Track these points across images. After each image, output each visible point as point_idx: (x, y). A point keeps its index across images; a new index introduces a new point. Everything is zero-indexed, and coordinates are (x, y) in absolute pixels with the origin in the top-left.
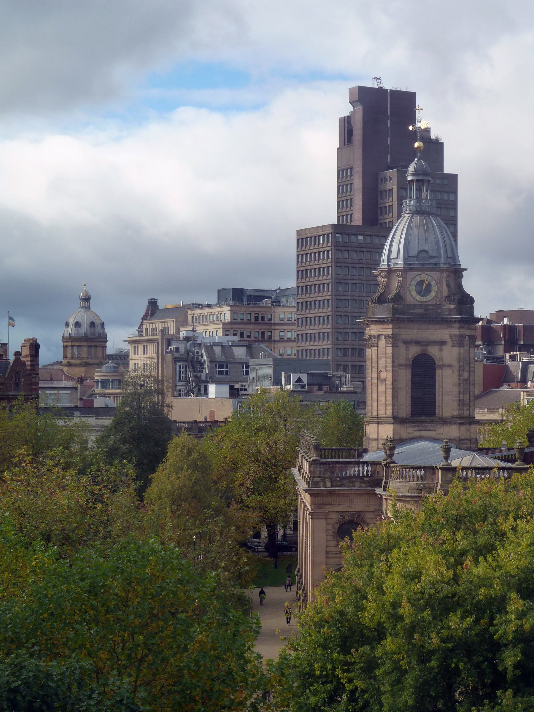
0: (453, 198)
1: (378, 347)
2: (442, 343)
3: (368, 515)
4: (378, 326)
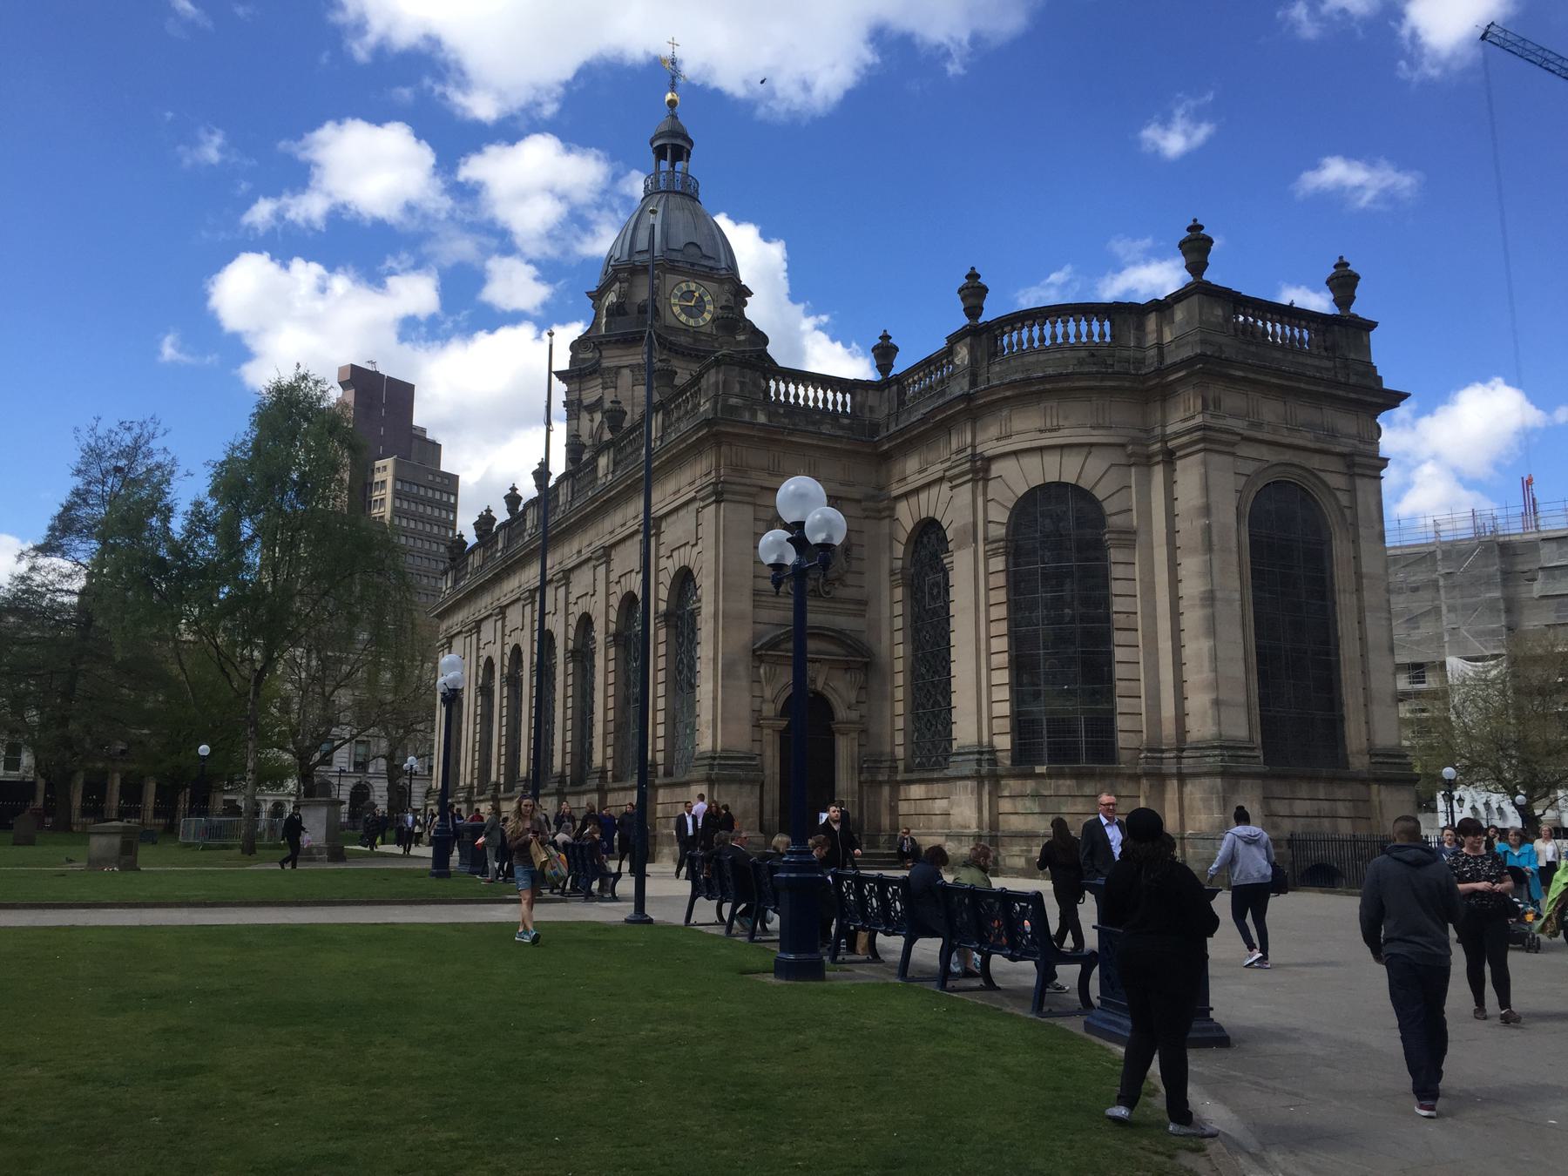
0: (452, 500)
1: (616, 388)
4: (617, 352)
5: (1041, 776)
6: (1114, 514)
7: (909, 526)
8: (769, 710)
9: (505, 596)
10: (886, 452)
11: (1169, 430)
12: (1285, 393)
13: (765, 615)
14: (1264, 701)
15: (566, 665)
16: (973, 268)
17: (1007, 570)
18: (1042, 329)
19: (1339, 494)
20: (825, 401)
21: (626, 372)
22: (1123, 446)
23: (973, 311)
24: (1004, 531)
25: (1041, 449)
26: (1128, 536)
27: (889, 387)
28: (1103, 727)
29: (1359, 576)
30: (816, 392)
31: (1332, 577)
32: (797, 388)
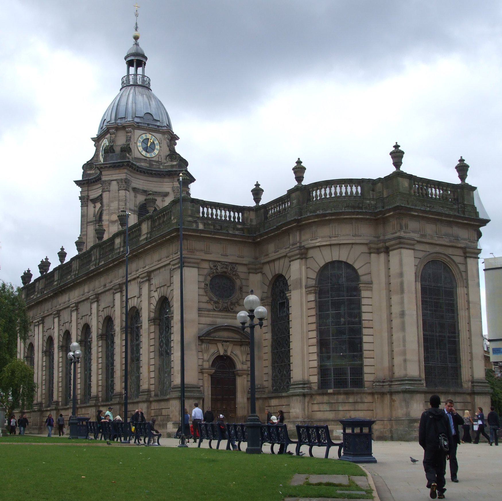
3: (241, 269)
5: (330, 394)
6: (363, 275)
7: (270, 277)
8: (206, 365)
9: (60, 305)
10: (259, 242)
11: (387, 237)
12: (435, 221)
13: (204, 320)
14: (426, 359)
15: (98, 341)
16: (299, 159)
17: (315, 301)
18: (330, 190)
19: (460, 266)
20: (230, 217)
21: (114, 183)
22: (366, 244)
23: (299, 178)
24: (314, 282)
25: (330, 245)
26: (369, 286)
27: (260, 210)
28: (358, 371)
29: (468, 302)
30: (225, 213)
31: (457, 303)
32: (217, 211)
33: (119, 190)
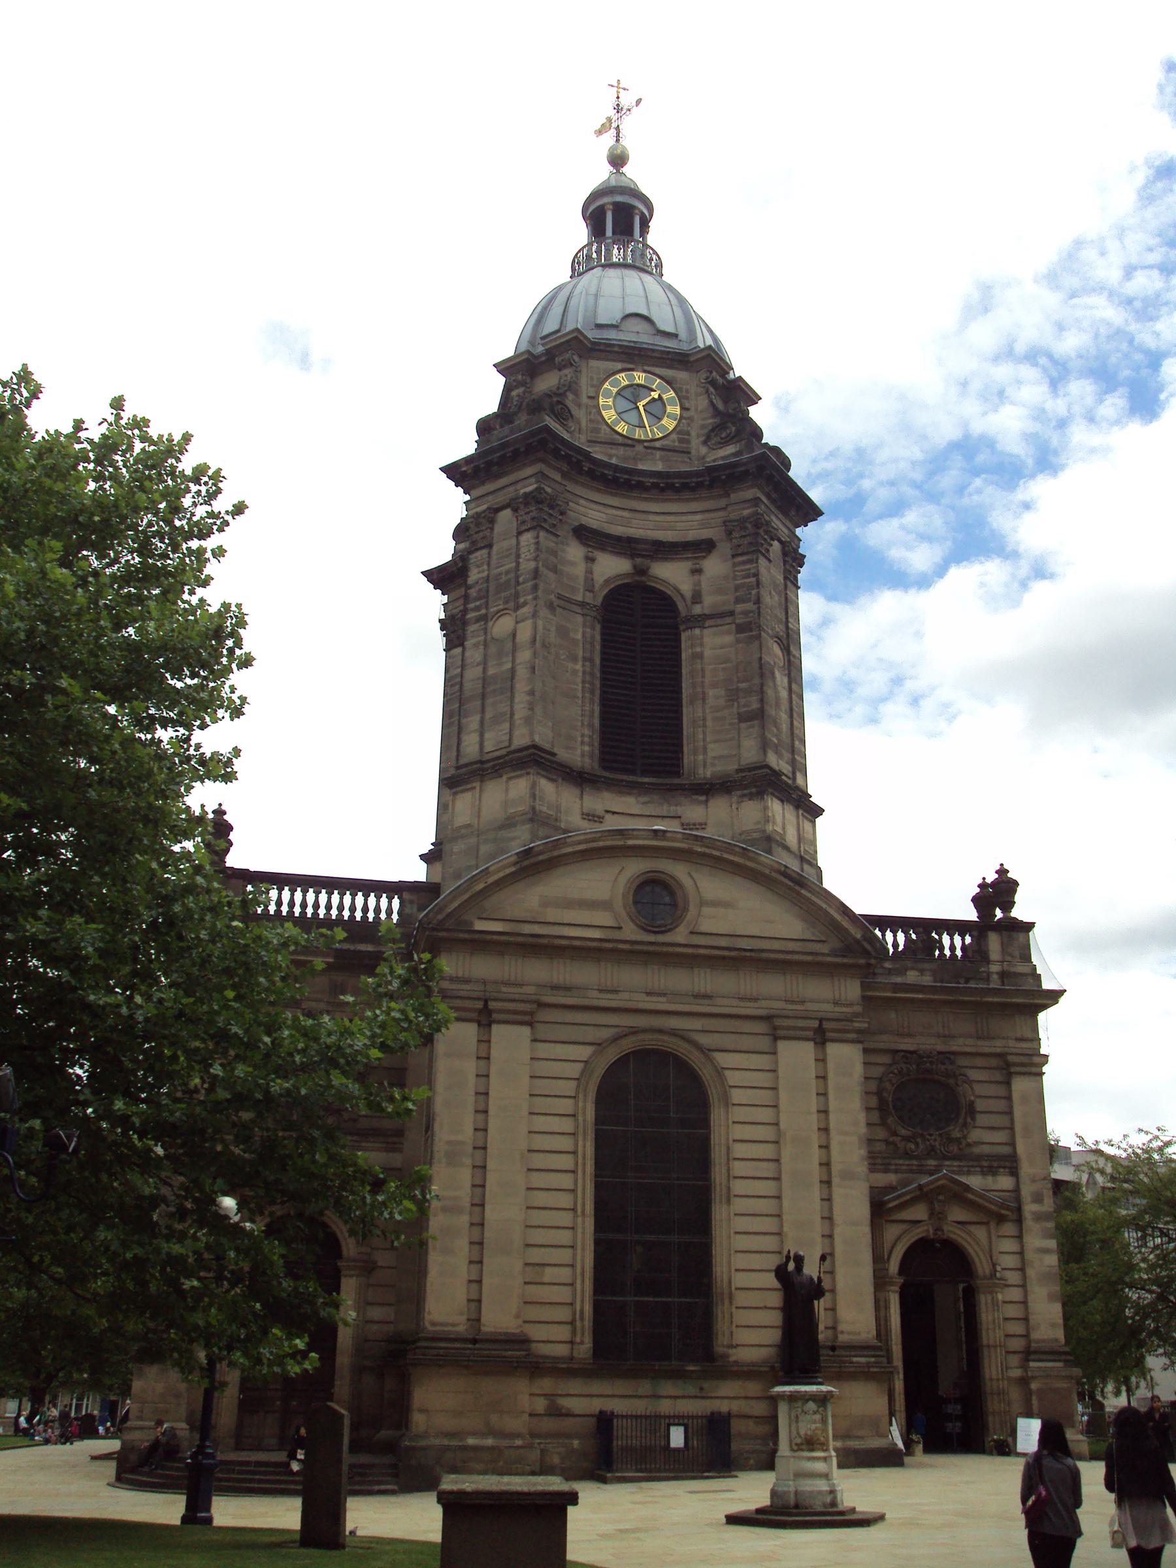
2: (705, 547)
33: (519, 533)
